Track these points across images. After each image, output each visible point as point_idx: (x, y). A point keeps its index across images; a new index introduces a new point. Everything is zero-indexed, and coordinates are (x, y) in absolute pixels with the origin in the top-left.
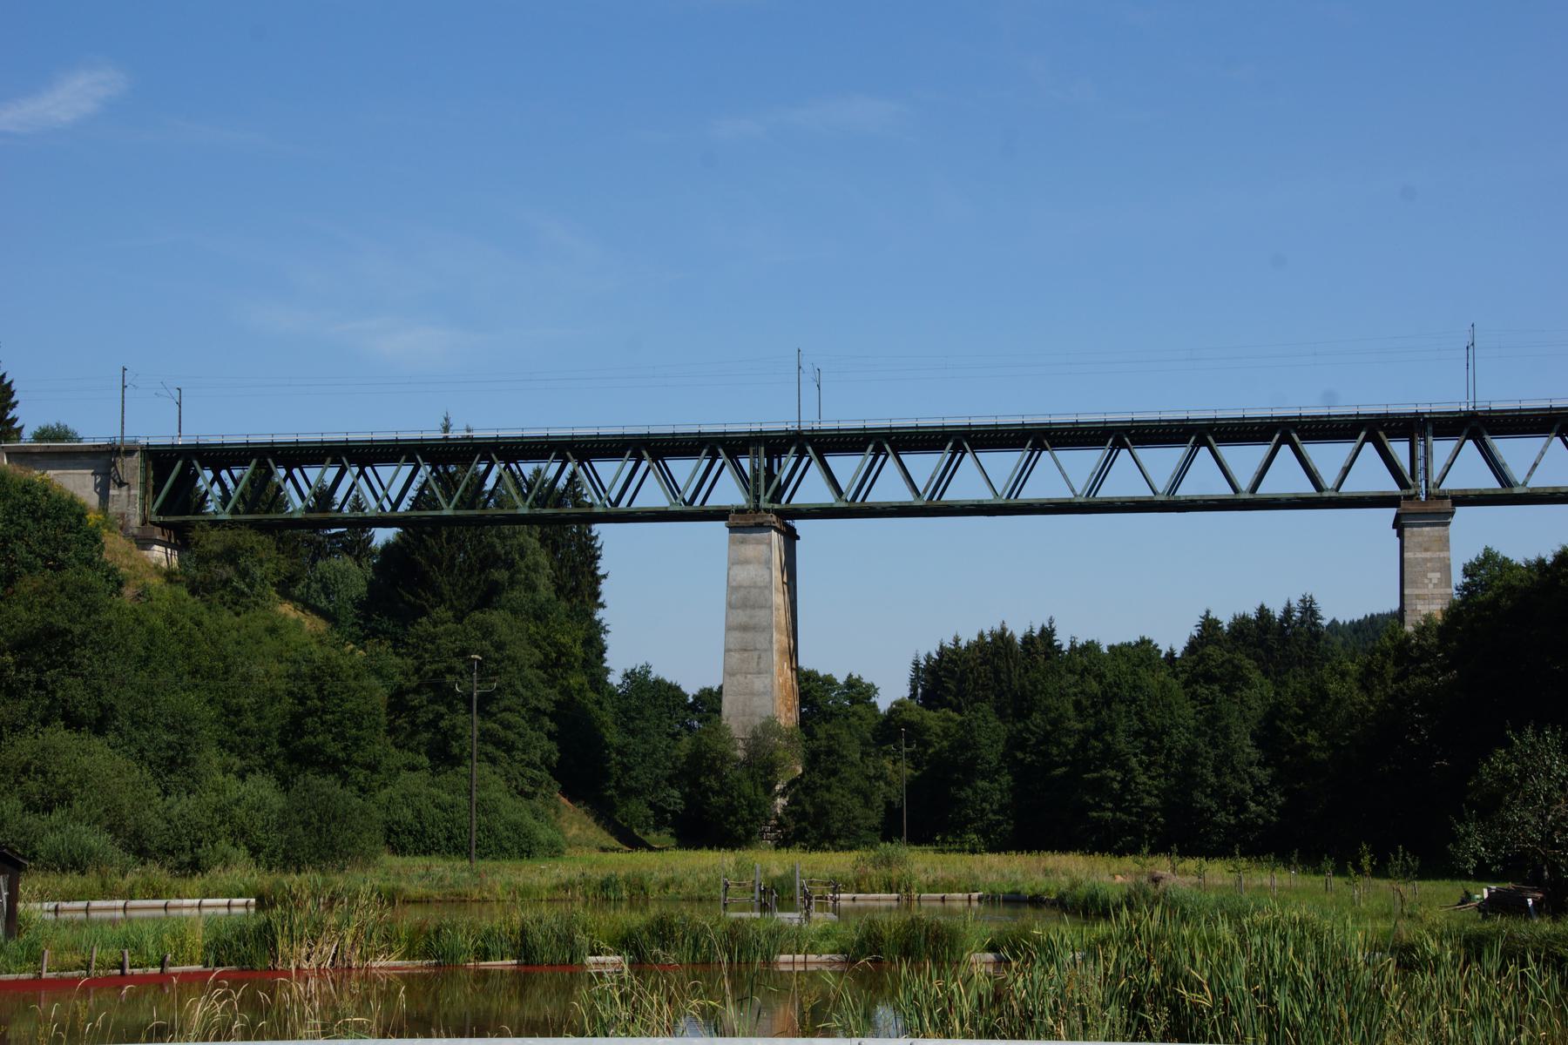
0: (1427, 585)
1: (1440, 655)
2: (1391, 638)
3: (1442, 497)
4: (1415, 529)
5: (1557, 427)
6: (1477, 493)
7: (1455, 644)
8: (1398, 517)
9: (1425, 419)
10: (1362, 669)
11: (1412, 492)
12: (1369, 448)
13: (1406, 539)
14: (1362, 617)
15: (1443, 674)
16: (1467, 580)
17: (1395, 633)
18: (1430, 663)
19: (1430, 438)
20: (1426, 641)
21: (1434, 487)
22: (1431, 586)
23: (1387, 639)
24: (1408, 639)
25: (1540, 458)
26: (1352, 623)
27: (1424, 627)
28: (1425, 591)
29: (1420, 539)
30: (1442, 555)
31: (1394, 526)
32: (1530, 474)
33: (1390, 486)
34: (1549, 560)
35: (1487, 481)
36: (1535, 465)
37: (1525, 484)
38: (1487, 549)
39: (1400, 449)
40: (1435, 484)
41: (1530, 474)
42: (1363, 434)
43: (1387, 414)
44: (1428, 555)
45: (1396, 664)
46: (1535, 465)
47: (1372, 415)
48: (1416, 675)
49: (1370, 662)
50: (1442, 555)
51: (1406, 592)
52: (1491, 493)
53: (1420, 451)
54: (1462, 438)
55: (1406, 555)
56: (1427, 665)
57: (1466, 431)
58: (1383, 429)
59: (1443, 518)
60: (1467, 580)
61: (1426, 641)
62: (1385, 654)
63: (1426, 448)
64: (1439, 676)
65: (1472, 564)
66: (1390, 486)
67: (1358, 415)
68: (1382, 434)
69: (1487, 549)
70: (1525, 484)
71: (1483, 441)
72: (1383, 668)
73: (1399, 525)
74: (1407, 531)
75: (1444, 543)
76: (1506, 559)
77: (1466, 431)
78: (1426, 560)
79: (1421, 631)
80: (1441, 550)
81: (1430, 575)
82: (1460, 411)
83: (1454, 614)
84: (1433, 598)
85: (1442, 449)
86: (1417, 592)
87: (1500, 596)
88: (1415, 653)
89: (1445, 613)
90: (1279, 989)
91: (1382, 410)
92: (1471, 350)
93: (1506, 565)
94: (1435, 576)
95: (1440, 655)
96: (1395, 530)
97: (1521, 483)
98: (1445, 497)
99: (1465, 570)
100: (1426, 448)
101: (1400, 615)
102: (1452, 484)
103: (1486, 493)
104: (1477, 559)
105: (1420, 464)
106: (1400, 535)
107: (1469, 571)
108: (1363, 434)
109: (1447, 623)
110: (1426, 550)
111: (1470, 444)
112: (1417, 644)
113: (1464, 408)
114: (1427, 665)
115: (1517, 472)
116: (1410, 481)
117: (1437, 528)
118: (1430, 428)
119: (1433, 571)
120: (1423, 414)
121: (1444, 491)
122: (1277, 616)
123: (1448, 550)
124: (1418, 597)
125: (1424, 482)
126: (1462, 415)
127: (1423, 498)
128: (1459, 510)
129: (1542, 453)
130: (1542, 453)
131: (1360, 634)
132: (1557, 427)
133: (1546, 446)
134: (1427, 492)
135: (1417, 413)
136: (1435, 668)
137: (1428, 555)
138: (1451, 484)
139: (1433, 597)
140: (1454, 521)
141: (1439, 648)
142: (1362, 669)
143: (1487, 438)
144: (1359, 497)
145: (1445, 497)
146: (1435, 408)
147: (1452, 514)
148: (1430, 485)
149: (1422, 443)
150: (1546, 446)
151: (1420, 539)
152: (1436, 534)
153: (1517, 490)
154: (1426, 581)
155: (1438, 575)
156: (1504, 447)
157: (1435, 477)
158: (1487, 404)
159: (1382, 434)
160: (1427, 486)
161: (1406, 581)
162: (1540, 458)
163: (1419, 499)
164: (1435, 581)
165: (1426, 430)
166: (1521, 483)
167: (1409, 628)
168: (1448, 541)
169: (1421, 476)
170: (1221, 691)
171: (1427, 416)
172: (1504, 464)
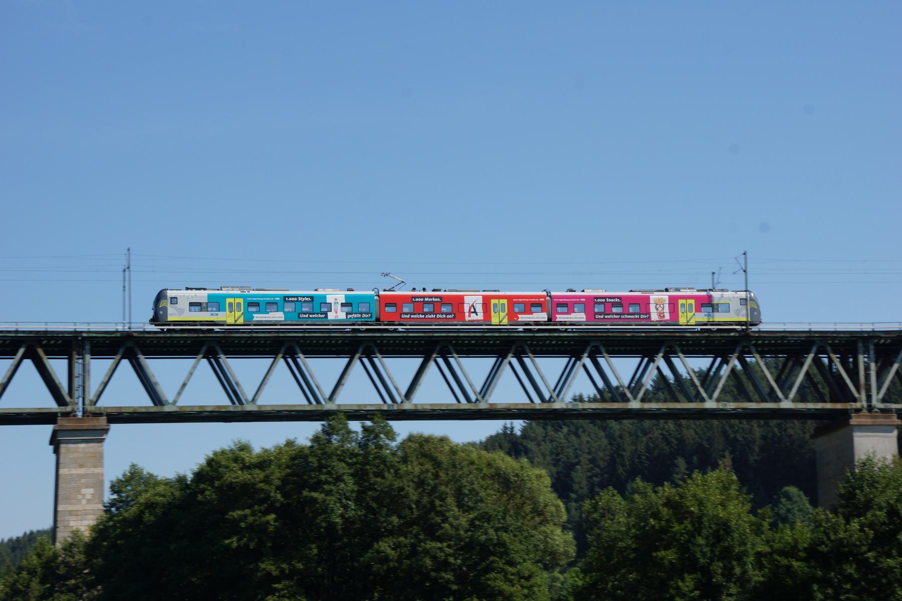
0: (80, 500)
1: (86, 571)
2: (39, 556)
3: (97, 414)
4: (71, 445)
5: (204, 349)
6: (131, 411)
7: (100, 560)
8: (55, 434)
9: (84, 338)
10: (8, 589)
11: (69, 409)
12: (28, 364)
13: (62, 456)
14: (21, 534)
15: (88, 590)
16: (115, 496)
17: (43, 550)
18: (76, 579)
19: (88, 357)
20: (73, 557)
21: (90, 405)
22: (84, 502)
23: (34, 557)
24: (55, 556)
25: (189, 378)
26: (10, 540)
27: (71, 544)
28: (78, 507)
29: (75, 455)
30: (96, 471)
31: (51, 443)
32: (179, 394)
33: (48, 403)
34: (190, 476)
35: (142, 400)
36: (184, 385)
37: (175, 402)
38: (133, 466)
39: (58, 367)
40: (91, 401)
41: (179, 394)
42: (21, 351)
43: (46, 332)
44: (82, 471)
45: (43, 582)
46: (184, 385)
47: (31, 332)
48: (62, 592)
49: (16, 581)
50: (96, 471)
51: (60, 508)
52: (144, 410)
53: (78, 369)
54: (118, 357)
55: (62, 471)
56: (73, 582)
57: (122, 351)
58: (42, 346)
59: (98, 435)
60: (115, 496)
61: (73, 557)
62: (32, 572)
63: (84, 365)
64: (84, 592)
65: (119, 481)
66: (48, 403)
67: (17, 332)
68: (40, 351)
69: (133, 466)
70: (175, 402)
71: (137, 360)
72: (28, 586)
73: (55, 441)
74: (63, 448)
75: (98, 460)
76: (151, 476)
77: (122, 351)
78: (81, 476)
79: (69, 548)
80: (95, 467)
81: (84, 491)
82: (117, 332)
83: (101, 531)
84: (86, 514)
85: (99, 367)
86: (71, 508)
87: (142, 512)
88: (62, 571)
89: (94, 529)
90: (550, 538)
91: (41, 327)
92: (127, 273)
93: (150, 481)
94: (89, 492)
95: (86, 571)
96: (52, 447)
97: (171, 401)
98: (100, 415)
99: (113, 487)
100: (84, 365)
101: (53, 533)
102: (110, 401)
103: (139, 410)
104: (124, 475)
105: (77, 382)
106: (56, 451)
107: (115, 489)
108: (21, 351)
109: (94, 540)
110: (81, 466)
111: (125, 363)
112: (63, 562)
113: (120, 328)
114: (73, 582)
115: (168, 392)
116: (68, 399)
117: (91, 445)
118: (88, 347)
119: (87, 487)
120: (82, 332)
121: (100, 408)
122: (189, 479)
123: (102, 466)
124: (71, 513)
125: (81, 400)
126: (118, 335)
127: (80, 414)
128: (114, 427)
129: (191, 374)
130: (191, 374)
131: (18, 552)
132: (204, 349)
133: (194, 367)
134: (83, 408)
135: (75, 332)
136: (80, 585)
137: (82, 471)
138: (104, 403)
139: (86, 513)
140: (109, 438)
141: (86, 564)
142: (8, 589)
143: (141, 357)
144: (17, 414)
145: (100, 415)
146: (94, 328)
147: (106, 431)
148: (87, 402)
149: (80, 361)
150: (194, 367)
151: (75, 455)
152: (91, 450)
153: (167, 409)
154: (80, 497)
155: (91, 491)
156: (156, 366)
157: (92, 393)
158: (141, 325)
159: (40, 351)
160: (84, 404)
161: (60, 498)
162: (189, 378)
163: (75, 416)
164: (88, 497)
165: (83, 348)
166: (171, 401)
167: (59, 545)
168: (102, 457)
169: (77, 393)
170: (259, 506)
171: (85, 335)
172: (156, 384)
